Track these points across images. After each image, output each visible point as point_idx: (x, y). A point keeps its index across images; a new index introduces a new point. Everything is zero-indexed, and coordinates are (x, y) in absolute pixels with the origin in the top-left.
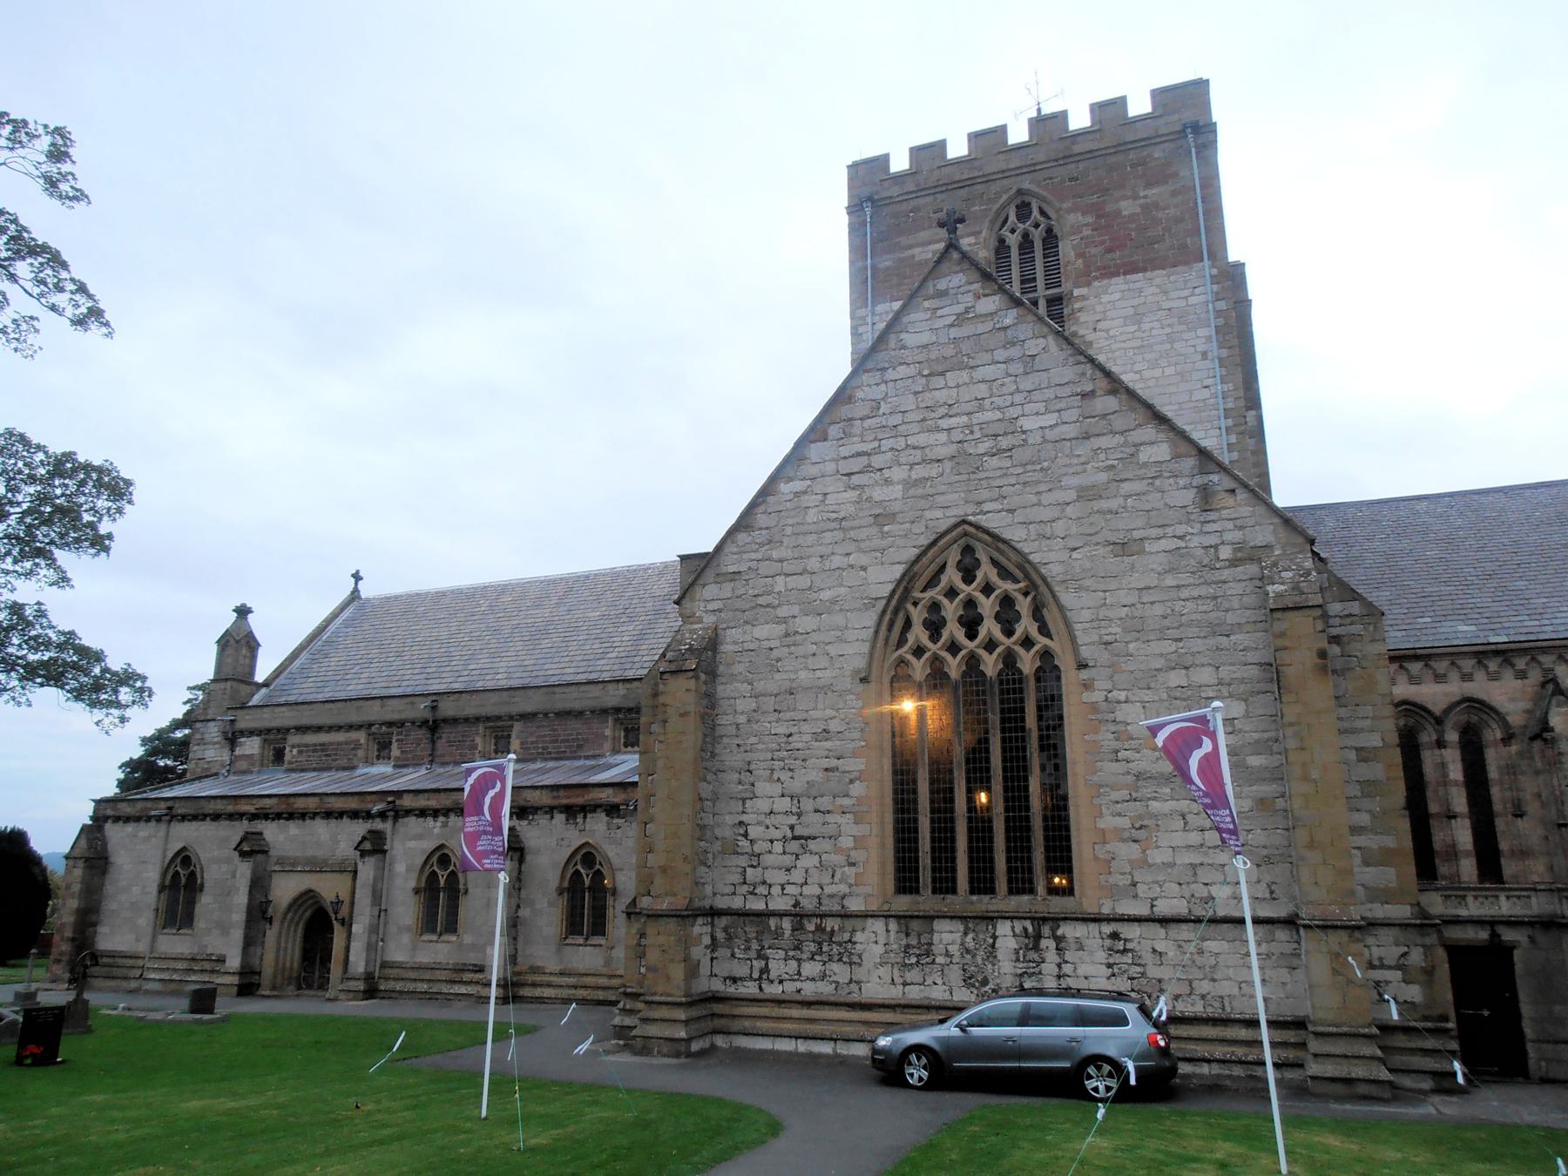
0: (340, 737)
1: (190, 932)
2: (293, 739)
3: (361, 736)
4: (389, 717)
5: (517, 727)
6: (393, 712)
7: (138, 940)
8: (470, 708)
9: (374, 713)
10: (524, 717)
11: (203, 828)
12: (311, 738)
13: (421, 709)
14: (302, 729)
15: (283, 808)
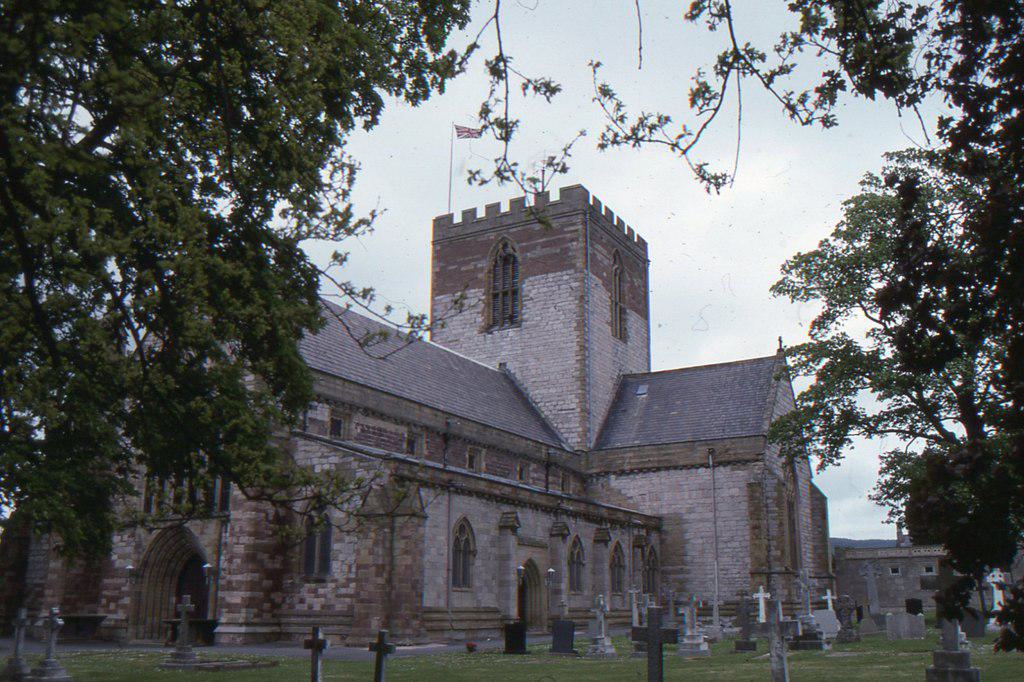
0: (390, 427)
1: (467, 589)
2: (358, 418)
3: (403, 430)
4: (425, 421)
5: (484, 451)
6: (427, 418)
7: (439, 597)
8: (468, 431)
9: (414, 414)
10: (490, 447)
11: (472, 502)
12: (372, 422)
13: (438, 423)
14: (368, 412)
15: (513, 496)
